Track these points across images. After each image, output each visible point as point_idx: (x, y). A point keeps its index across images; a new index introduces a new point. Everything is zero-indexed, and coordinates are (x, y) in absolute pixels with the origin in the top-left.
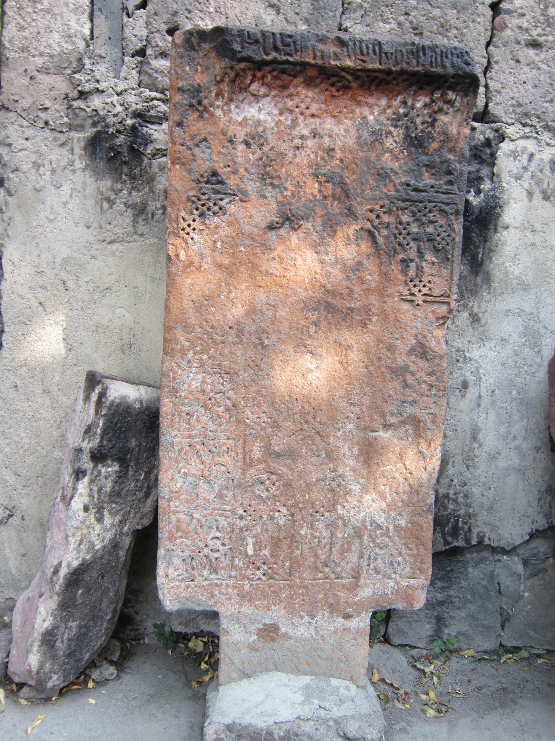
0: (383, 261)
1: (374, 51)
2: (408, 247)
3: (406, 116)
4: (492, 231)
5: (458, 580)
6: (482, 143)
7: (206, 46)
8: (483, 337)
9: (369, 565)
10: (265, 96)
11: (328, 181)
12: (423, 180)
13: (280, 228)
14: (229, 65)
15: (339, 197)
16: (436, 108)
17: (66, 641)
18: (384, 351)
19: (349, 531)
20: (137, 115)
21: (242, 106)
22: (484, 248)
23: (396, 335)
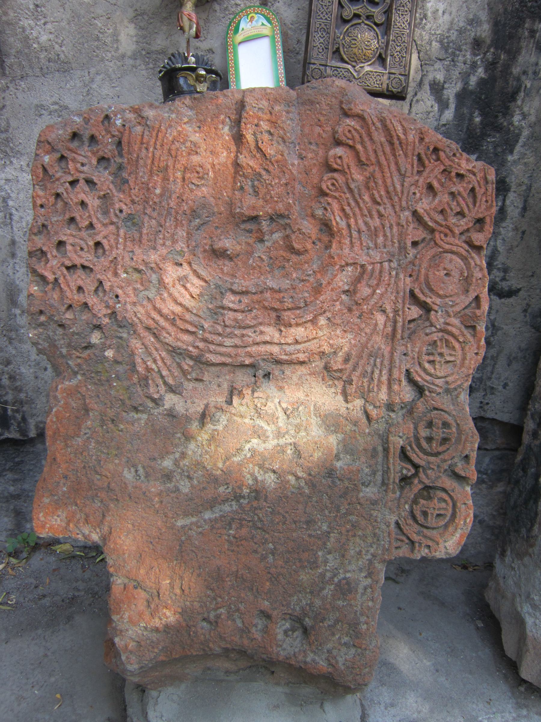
5: (31, 473)
8: (8, 150)
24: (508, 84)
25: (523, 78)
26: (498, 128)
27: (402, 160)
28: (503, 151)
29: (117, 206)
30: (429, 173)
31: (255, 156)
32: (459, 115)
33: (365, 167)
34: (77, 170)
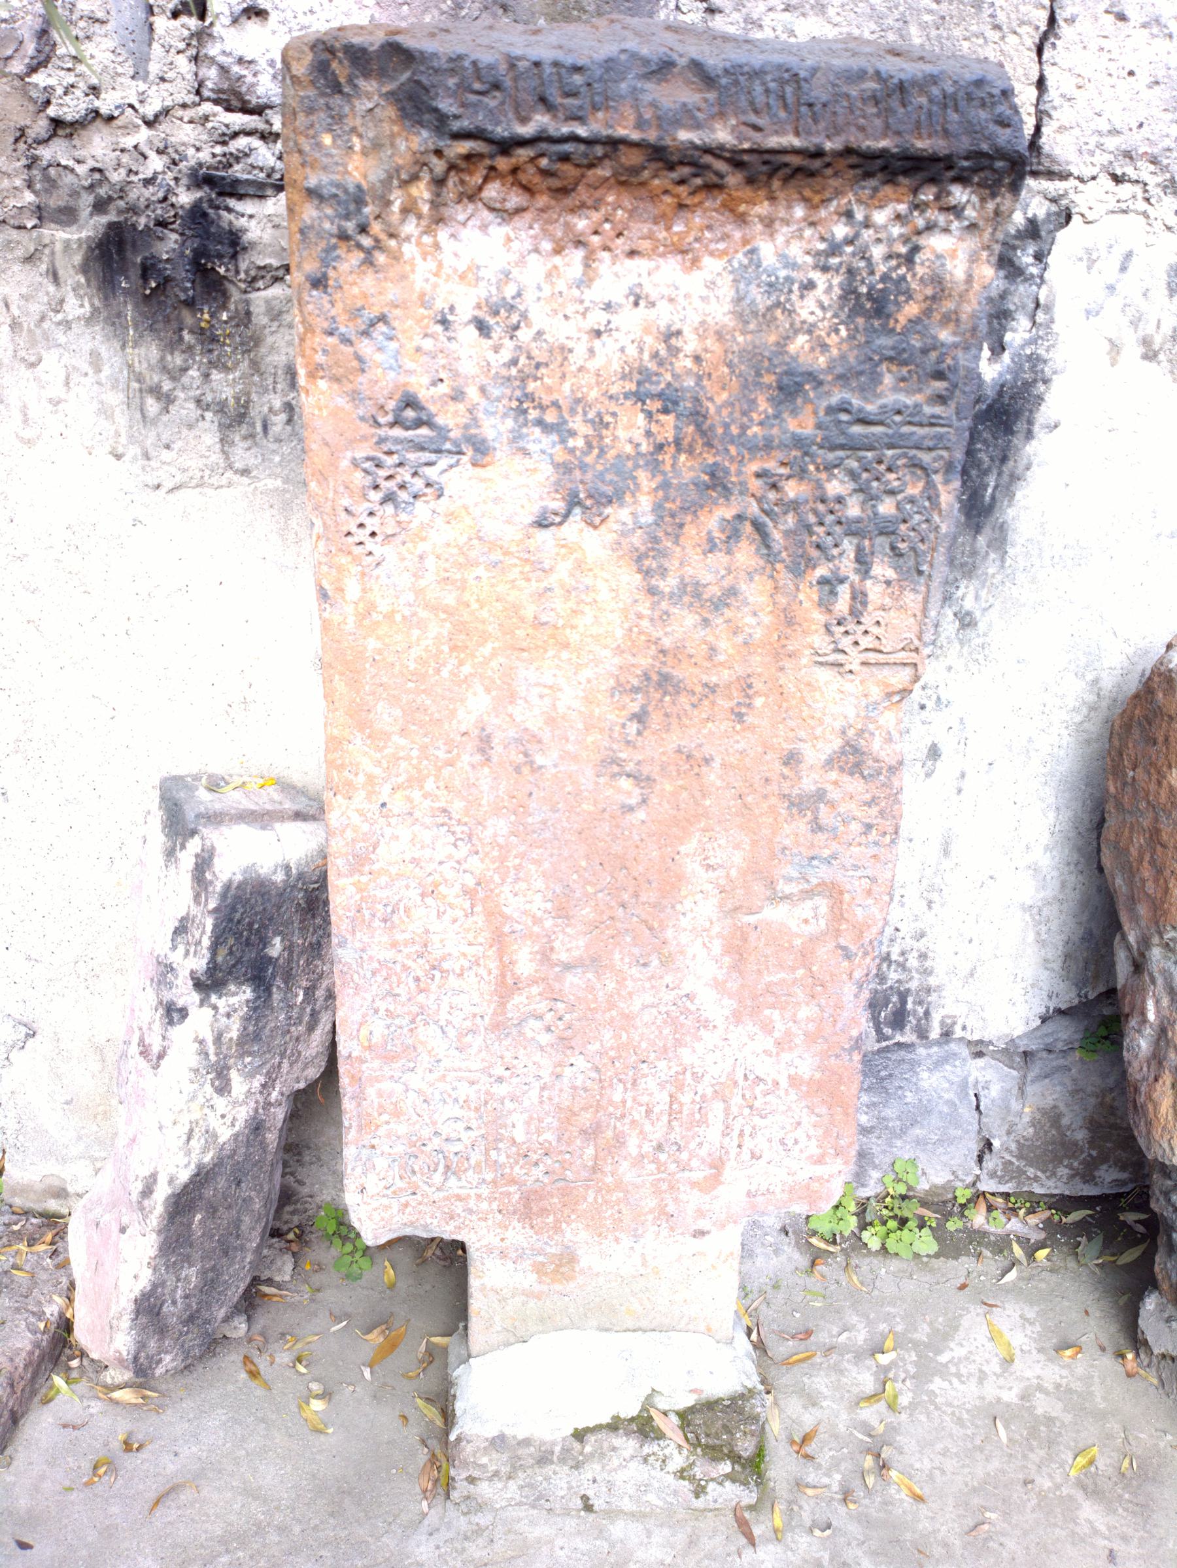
0: (781, 583)
1: (783, 98)
2: (835, 552)
3: (850, 242)
4: (1021, 436)
6: (1018, 231)
7: (368, 85)
9: (740, 1146)
10: (519, 211)
11: (665, 411)
12: (879, 396)
13: (561, 524)
14: (432, 147)
15: (690, 446)
16: (920, 223)
17: (179, 1301)
18: (777, 766)
19: (705, 1088)
20: (202, 179)
21: (465, 233)
22: (1000, 474)
23: (802, 734)
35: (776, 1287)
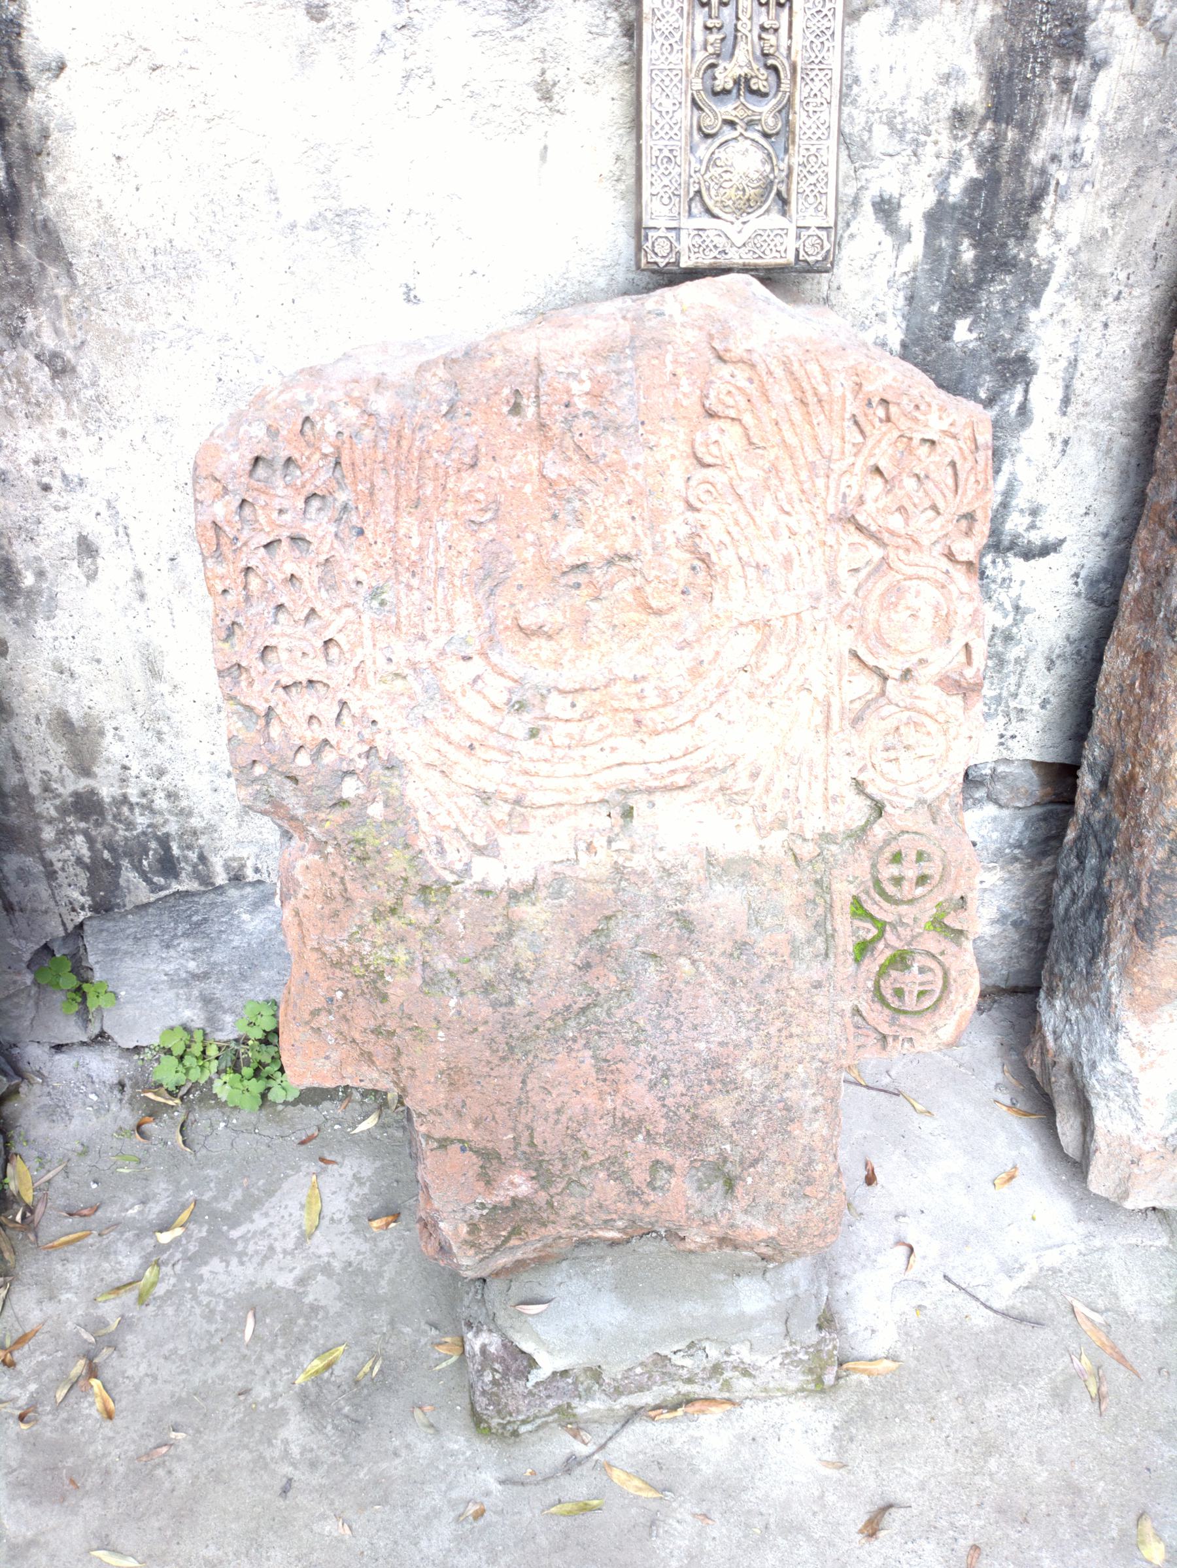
24: (1023, 183)
25: (1052, 169)
26: (1005, 264)
27: (823, 431)
28: (1021, 306)
29: (351, 577)
30: (873, 447)
31: (570, 459)
32: (932, 251)
33: (760, 451)
34: (272, 523)
35: (85, 1152)
